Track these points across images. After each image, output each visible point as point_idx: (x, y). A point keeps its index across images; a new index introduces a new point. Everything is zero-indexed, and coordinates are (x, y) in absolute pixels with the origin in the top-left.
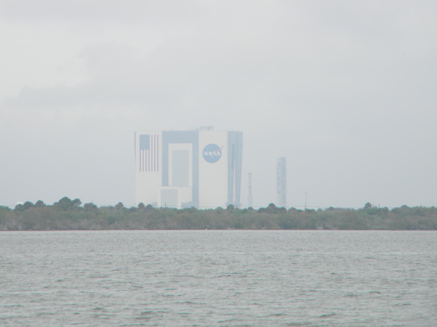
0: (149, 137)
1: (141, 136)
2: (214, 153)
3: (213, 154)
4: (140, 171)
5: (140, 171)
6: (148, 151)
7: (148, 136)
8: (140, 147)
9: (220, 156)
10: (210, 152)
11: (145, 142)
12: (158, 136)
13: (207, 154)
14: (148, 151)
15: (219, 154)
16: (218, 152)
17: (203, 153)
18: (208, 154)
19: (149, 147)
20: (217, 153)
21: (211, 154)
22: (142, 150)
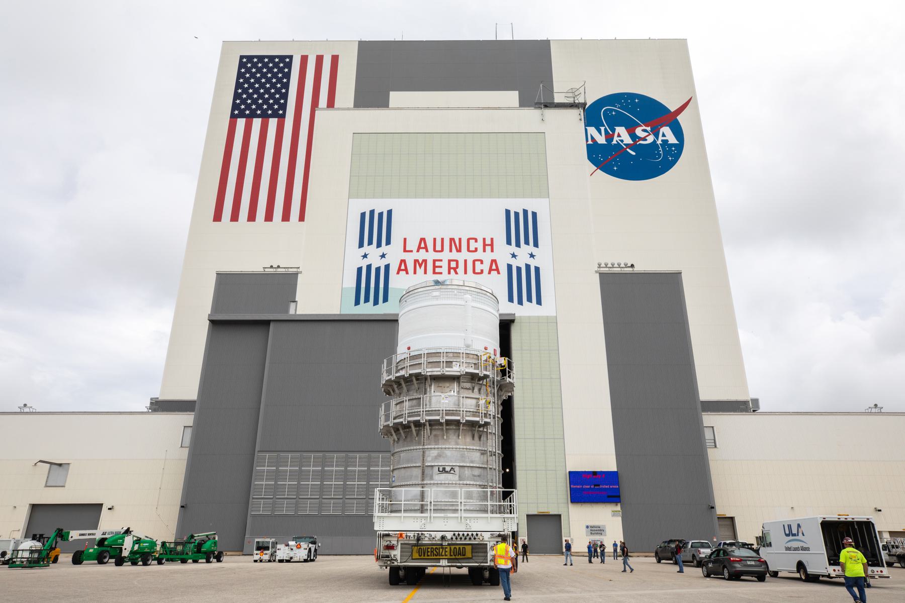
0: (289, 65)
2: (639, 132)
4: (218, 217)
5: (218, 217)
6: (273, 123)
7: (286, 61)
8: (235, 106)
9: (680, 147)
10: (621, 130)
11: (261, 85)
12: (335, 59)
14: (273, 123)
15: (672, 140)
16: (666, 130)
19: (284, 107)
20: (656, 133)
21: (628, 140)
22: (241, 123)
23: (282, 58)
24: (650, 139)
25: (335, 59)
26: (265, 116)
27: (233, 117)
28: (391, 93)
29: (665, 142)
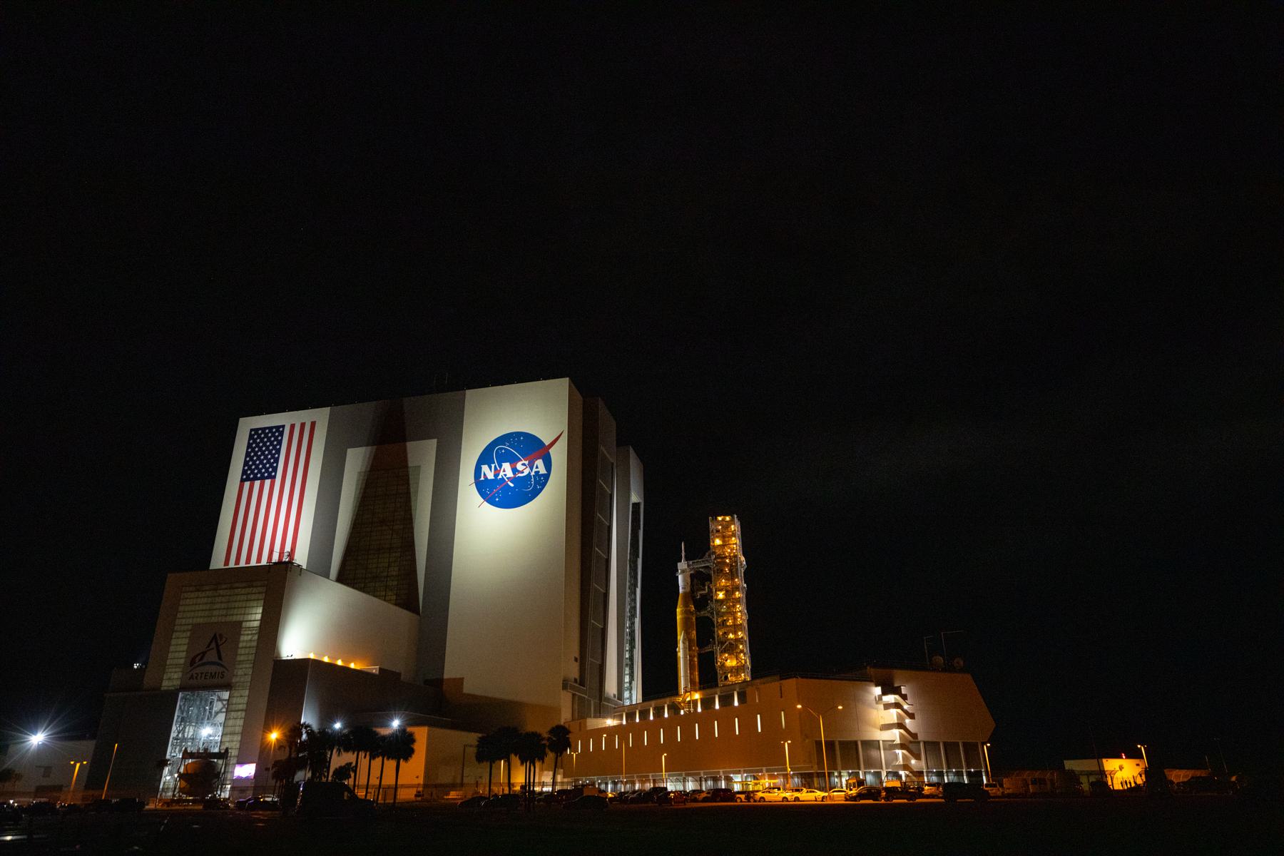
0: (281, 434)
1: (254, 433)
2: (519, 466)
3: (515, 470)
6: (268, 482)
7: (280, 429)
8: (244, 472)
9: (547, 477)
10: (506, 466)
12: (313, 424)
13: (491, 476)
15: (543, 471)
16: (539, 463)
17: (478, 471)
18: (496, 475)
19: (275, 469)
21: (510, 474)
22: (247, 484)
23: (278, 428)
24: (527, 472)
25: (313, 424)
26: (263, 479)
27: (242, 481)
28: (349, 451)
29: (537, 473)
